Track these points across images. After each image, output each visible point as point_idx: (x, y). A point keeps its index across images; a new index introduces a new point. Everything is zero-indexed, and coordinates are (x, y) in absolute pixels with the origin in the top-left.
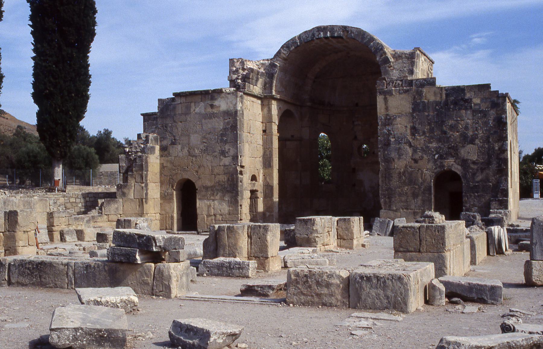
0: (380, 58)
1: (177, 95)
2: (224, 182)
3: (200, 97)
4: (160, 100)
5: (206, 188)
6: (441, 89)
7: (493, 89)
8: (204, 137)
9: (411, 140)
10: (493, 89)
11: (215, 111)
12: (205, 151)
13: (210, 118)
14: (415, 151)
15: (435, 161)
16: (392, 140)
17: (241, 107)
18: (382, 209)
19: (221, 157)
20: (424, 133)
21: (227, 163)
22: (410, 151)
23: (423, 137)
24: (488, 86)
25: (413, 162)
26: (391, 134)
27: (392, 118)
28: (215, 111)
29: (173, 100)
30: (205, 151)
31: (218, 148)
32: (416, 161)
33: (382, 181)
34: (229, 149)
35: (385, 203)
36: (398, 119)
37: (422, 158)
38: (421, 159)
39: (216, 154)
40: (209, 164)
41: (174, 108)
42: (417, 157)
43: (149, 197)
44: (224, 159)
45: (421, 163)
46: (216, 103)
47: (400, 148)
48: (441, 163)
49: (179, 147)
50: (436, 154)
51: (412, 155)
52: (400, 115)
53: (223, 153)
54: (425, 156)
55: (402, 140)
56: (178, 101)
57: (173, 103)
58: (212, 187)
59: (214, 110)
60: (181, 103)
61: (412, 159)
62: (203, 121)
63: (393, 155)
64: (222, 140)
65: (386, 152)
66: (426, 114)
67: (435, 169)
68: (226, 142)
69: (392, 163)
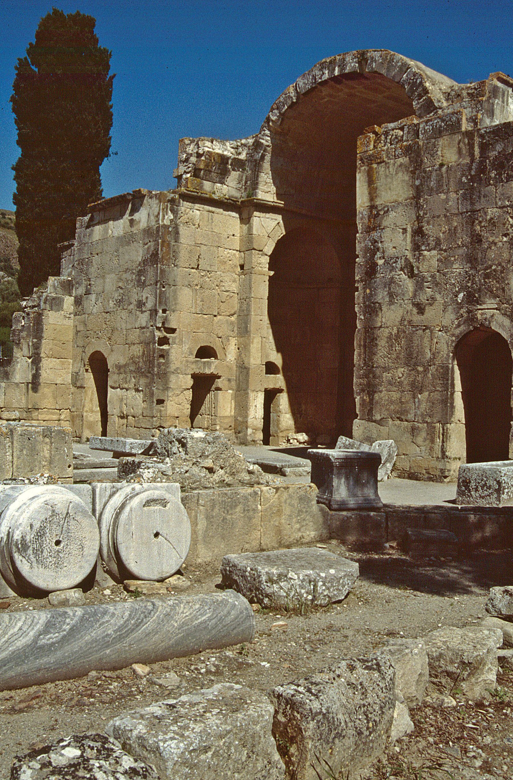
9: (411, 260)
14: (419, 287)
16: (381, 262)
17: (171, 221)
18: (356, 416)
23: (434, 252)
25: (415, 311)
26: (378, 249)
27: (382, 213)
32: (421, 310)
33: (360, 355)
34: (147, 298)
35: (363, 403)
38: (431, 305)
39: (131, 307)
42: (422, 298)
43: (42, 380)
45: (430, 312)
47: (392, 281)
48: (469, 312)
50: (459, 292)
51: (415, 296)
54: (438, 296)
55: (396, 262)
61: (414, 304)
63: (382, 296)
65: (368, 291)
66: (443, 196)
67: (459, 326)
69: (377, 315)
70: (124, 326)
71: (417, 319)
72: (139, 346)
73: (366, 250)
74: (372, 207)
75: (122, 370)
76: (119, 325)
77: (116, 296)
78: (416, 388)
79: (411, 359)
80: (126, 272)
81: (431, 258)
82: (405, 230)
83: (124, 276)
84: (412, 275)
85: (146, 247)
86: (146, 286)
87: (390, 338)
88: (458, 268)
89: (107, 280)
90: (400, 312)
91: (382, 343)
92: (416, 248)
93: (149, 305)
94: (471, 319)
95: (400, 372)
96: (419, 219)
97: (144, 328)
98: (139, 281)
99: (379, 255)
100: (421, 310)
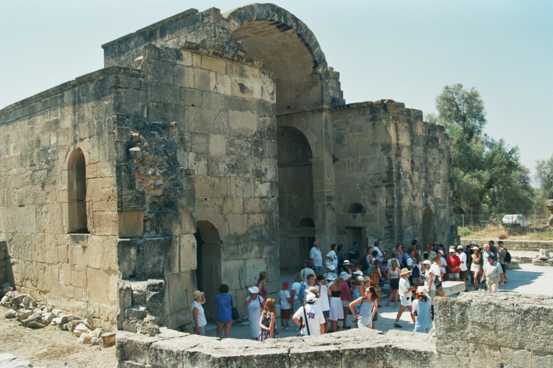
0: (322, 71)
2: (261, 226)
5: (237, 239)
8: (231, 144)
11: (246, 96)
14: (413, 189)
16: (402, 173)
19: (257, 182)
21: (264, 194)
23: (417, 173)
28: (246, 96)
30: (233, 168)
34: (266, 169)
39: (248, 175)
40: (240, 194)
41: (181, 73)
42: (414, 193)
44: (261, 186)
46: (248, 83)
53: (259, 175)
57: (178, 62)
58: (244, 235)
60: (192, 66)
62: (230, 112)
63: (403, 192)
70: (240, 194)
72: (261, 215)
74: (398, 144)
75: (241, 241)
76: (233, 193)
77: (228, 160)
80: (239, 137)
82: (408, 160)
83: (237, 141)
85: (261, 119)
86: (264, 158)
87: (406, 212)
89: (212, 141)
91: (404, 214)
92: (412, 170)
95: (410, 228)
96: (413, 156)
97: (265, 197)
98: (256, 151)
99: (401, 169)
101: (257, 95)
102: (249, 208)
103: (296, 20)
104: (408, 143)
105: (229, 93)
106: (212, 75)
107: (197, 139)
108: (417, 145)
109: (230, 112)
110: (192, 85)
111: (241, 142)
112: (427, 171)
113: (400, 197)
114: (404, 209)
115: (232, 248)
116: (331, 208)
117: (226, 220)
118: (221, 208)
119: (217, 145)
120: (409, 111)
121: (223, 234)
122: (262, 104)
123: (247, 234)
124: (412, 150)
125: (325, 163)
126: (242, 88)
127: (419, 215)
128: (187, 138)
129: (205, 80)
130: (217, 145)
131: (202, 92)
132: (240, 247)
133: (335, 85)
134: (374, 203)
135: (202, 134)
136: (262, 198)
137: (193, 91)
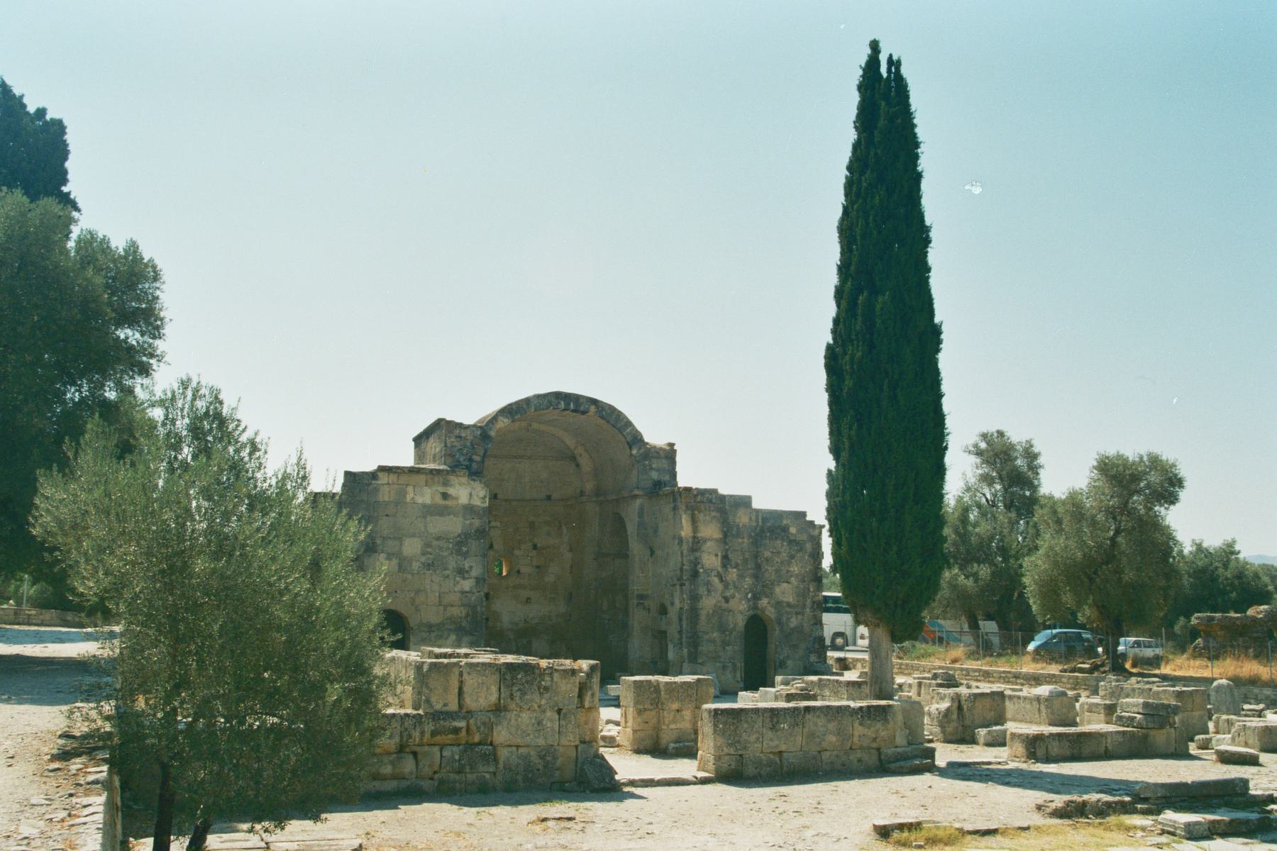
1: (382, 469)
3: (423, 477)
4: (348, 474)
5: (430, 627)
6: (757, 511)
7: (808, 518)
8: (428, 545)
10: (808, 518)
11: (449, 503)
12: (429, 566)
13: (441, 514)
14: (726, 586)
15: (749, 600)
20: (737, 566)
21: (467, 589)
22: (720, 586)
24: (803, 514)
28: (449, 503)
29: (373, 475)
31: (452, 564)
35: (690, 654)
36: (709, 544)
37: (733, 597)
39: (447, 572)
40: (436, 588)
41: (376, 490)
42: (728, 594)
46: (451, 491)
49: (383, 556)
52: (710, 539)
53: (462, 572)
56: (384, 478)
59: (447, 502)
63: (702, 590)
64: (459, 552)
68: (465, 555)
71: (724, 605)
73: (691, 562)
74: (694, 537)
78: (725, 644)
79: (722, 628)
80: (438, 539)
81: (733, 574)
83: (435, 543)
84: (721, 580)
87: (708, 615)
88: (749, 580)
90: (714, 601)
91: (703, 618)
92: (724, 566)
93: (474, 573)
94: (755, 607)
100: (727, 600)
101: (464, 500)
102: (445, 602)
103: (594, 402)
104: (718, 535)
105: (428, 501)
106: (410, 489)
107: (390, 543)
108: (738, 535)
109: (428, 519)
110: (386, 499)
111: (441, 543)
112: (758, 567)
113: (695, 598)
114: (703, 613)
115: (424, 635)
116: (644, 608)
117: (417, 610)
118: (413, 600)
119: (412, 547)
120: (723, 497)
121: (413, 621)
122: (469, 510)
123: (442, 624)
124: (726, 543)
125: (637, 559)
126: (445, 496)
127: (741, 621)
128: (378, 542)
129: (402, 493)
130: (412, 547)
131: (397, 503)
132: (433, 635)
133: (666, 466)
134: (672, 604)
135: (395, 538)
136: (463, 592)
137: (387, 504)
